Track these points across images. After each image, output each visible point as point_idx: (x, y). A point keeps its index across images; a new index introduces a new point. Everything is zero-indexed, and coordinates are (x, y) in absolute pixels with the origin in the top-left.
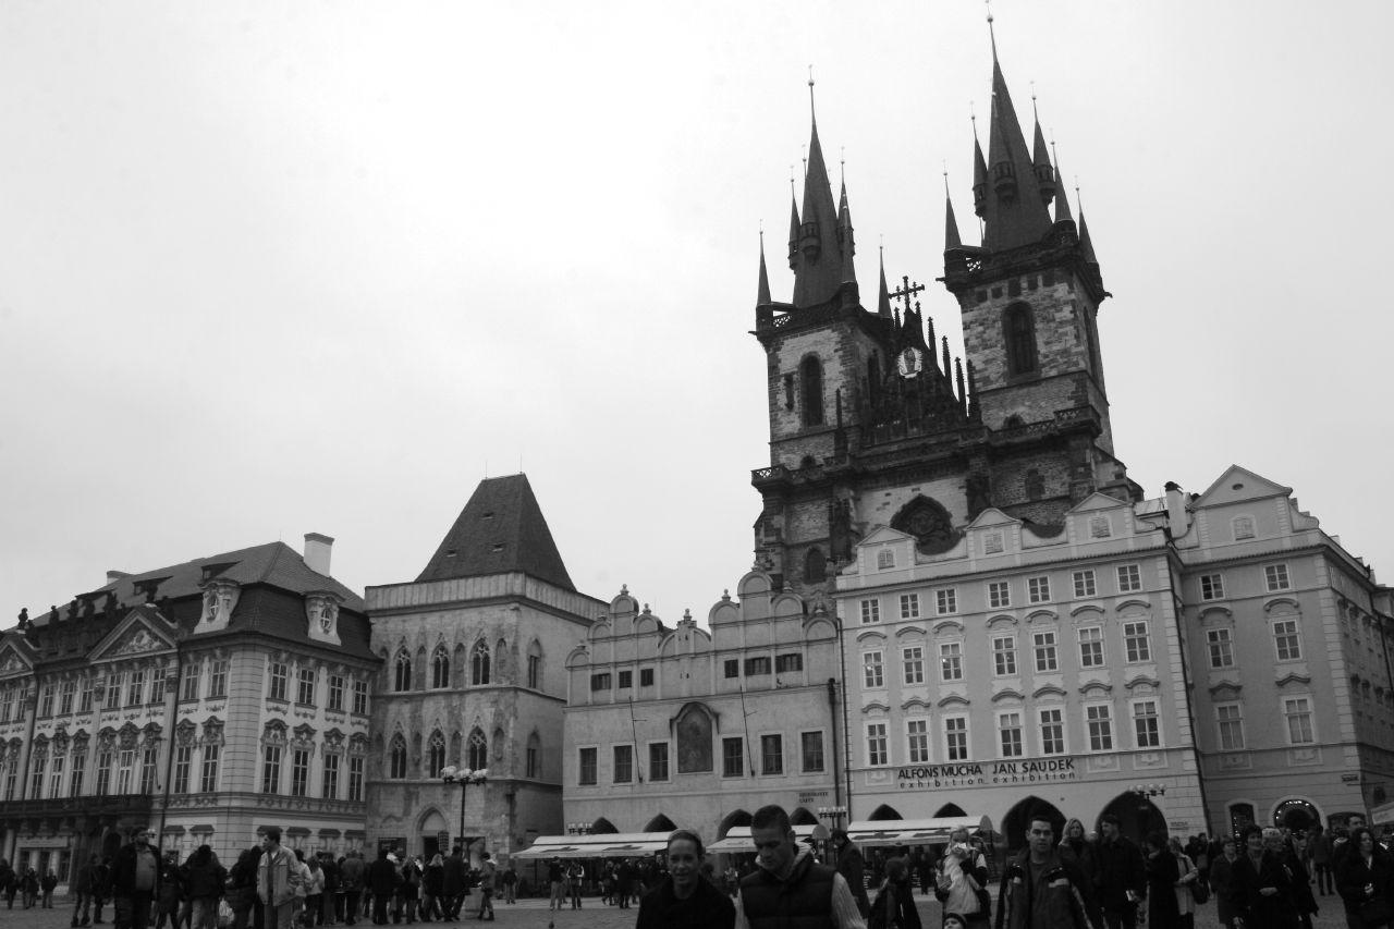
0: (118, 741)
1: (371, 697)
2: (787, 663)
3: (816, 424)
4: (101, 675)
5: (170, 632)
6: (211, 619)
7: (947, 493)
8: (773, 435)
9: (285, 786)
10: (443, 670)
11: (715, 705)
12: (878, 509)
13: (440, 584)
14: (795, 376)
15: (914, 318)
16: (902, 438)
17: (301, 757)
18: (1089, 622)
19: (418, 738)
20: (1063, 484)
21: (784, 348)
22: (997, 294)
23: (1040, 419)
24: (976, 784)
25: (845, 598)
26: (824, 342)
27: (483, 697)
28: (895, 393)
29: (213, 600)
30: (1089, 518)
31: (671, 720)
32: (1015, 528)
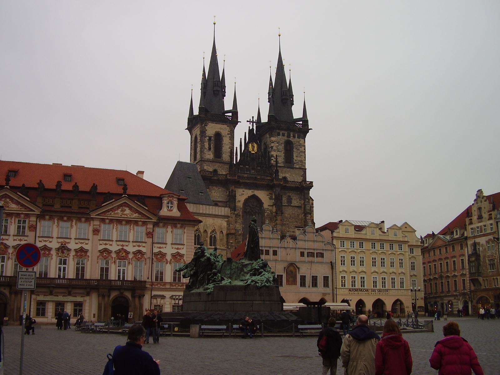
3: (217, 158)
7: (263, 195)
8: (201, 157)
11: (298, 265)
12: (240, 195)
13: (198, 205)
14: (212, 138)
16: (248, 173)
18: (392, 256)
20: (297, 202)
21: (208, 126)
22: (283, 135)
23: (292, 180)
24: (367, 294)
25: (336, 239)
26: (223, 129)
28: (247, 157)
30: (393, 231)
31: (285, 268)
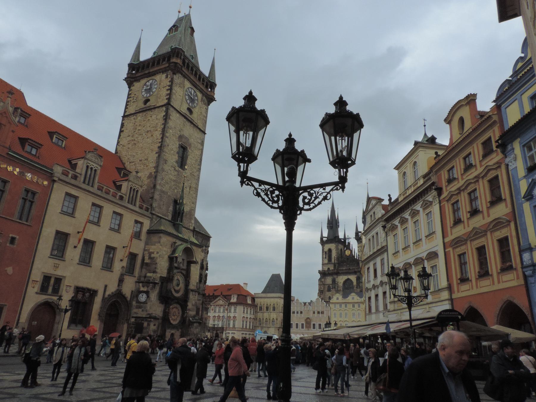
0: (216, 318)
1: (256, 312)
2: (323, 313)
4: (213, 306)
5: (227, 302)
6: (233, 300)
7: (353, 278)
8: (322, 263)
9: (244, 327)
10: (267, 308)
15: (349, 243)
17: (246, 322)
19: (263, 319)
26: (332, 246)
27: (274, 313)
29: (233, 297)
32: (356, 296)
